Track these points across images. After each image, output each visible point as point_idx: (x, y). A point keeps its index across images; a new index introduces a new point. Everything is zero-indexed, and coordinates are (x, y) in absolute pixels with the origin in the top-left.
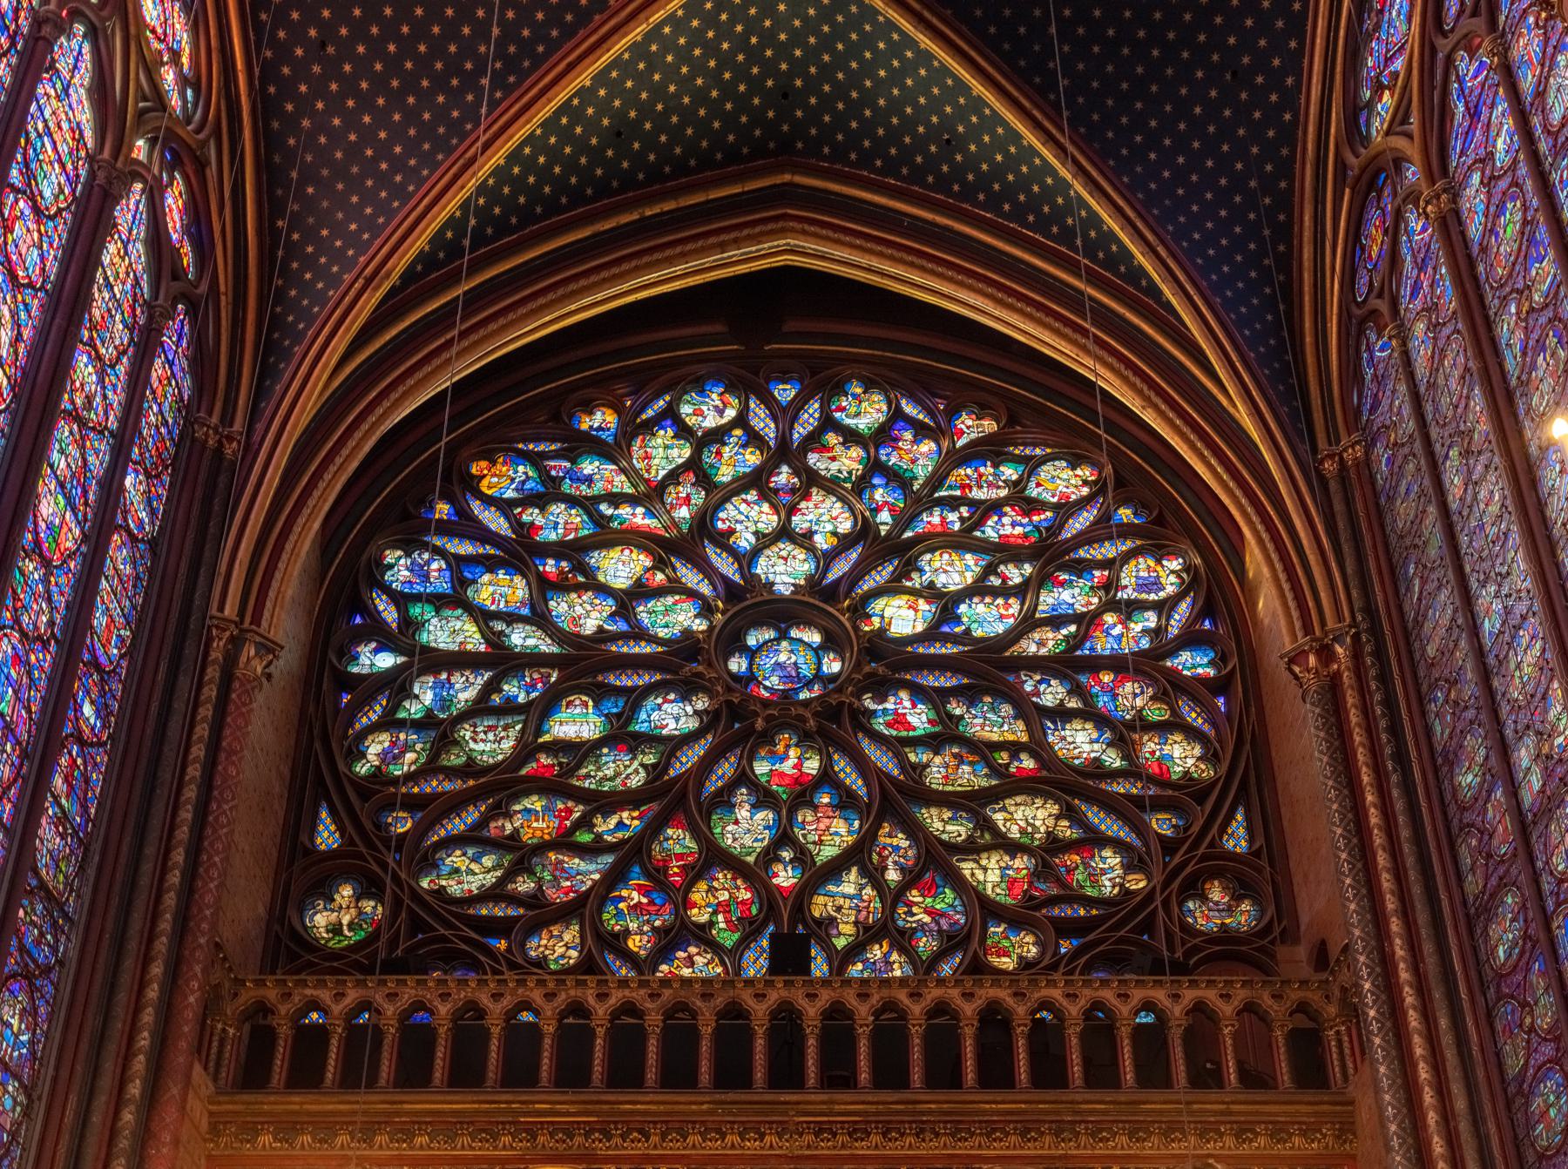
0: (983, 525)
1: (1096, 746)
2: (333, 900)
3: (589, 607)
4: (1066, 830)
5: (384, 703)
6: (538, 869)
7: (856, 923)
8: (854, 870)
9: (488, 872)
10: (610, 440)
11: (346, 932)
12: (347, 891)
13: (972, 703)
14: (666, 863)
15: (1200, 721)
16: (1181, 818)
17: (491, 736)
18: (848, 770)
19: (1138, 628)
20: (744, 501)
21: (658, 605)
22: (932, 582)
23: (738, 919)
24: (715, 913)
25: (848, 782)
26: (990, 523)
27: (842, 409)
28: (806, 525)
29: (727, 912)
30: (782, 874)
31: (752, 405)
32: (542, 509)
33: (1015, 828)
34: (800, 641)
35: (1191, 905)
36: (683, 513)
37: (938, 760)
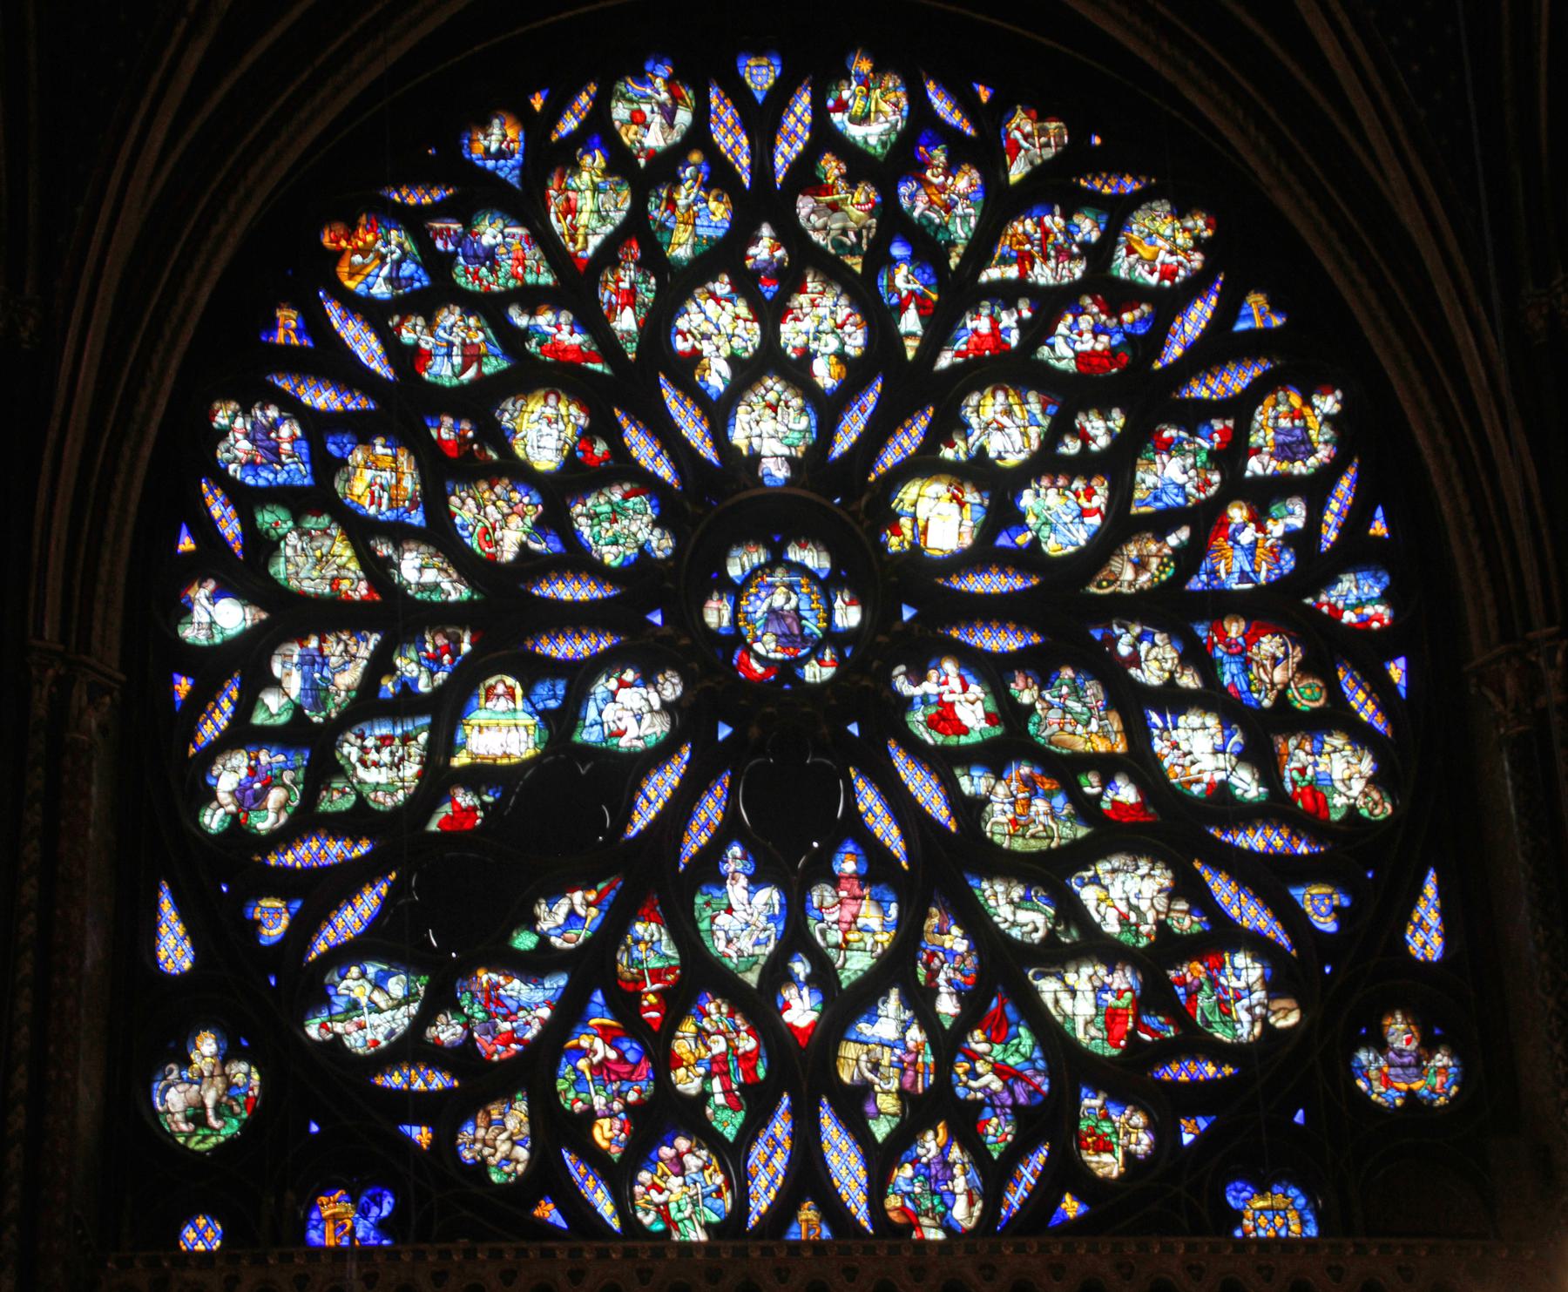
0: (1051, 331)
1: (1221, 761)
2: (188, 1063)
3: (506, 510)
4: (1186, 923)
5: (235, 695)
6: (465, 1002)
7: (902, 1094)
8: (894, 994)
9: (398, 1006)
10: (514, 180)
11: (212, 1121)
12: (207, 1046)
13: (1045, 683)
14: (639, 982)
15: (1370, 707)
16: (1346, 894)
17: (385, 756)
18: (878, 809)
19: (1276, 529)
20: (713, 295)
21: (598, 503)
22: (982, 450)
23: (741, 1087)
24: (708, 1077)
25: (878, 832)
26: (1062, 328)
27: (842, 106)
28: (800, 341)
29: (724, 1074)
30: (795, 1002)
31: (714, 102)
32: (431, 325)
33: (1112, 916)
34: (801, 568)
35: (1364, 1056)
36: (626, 322)
37: (1001, 789)
